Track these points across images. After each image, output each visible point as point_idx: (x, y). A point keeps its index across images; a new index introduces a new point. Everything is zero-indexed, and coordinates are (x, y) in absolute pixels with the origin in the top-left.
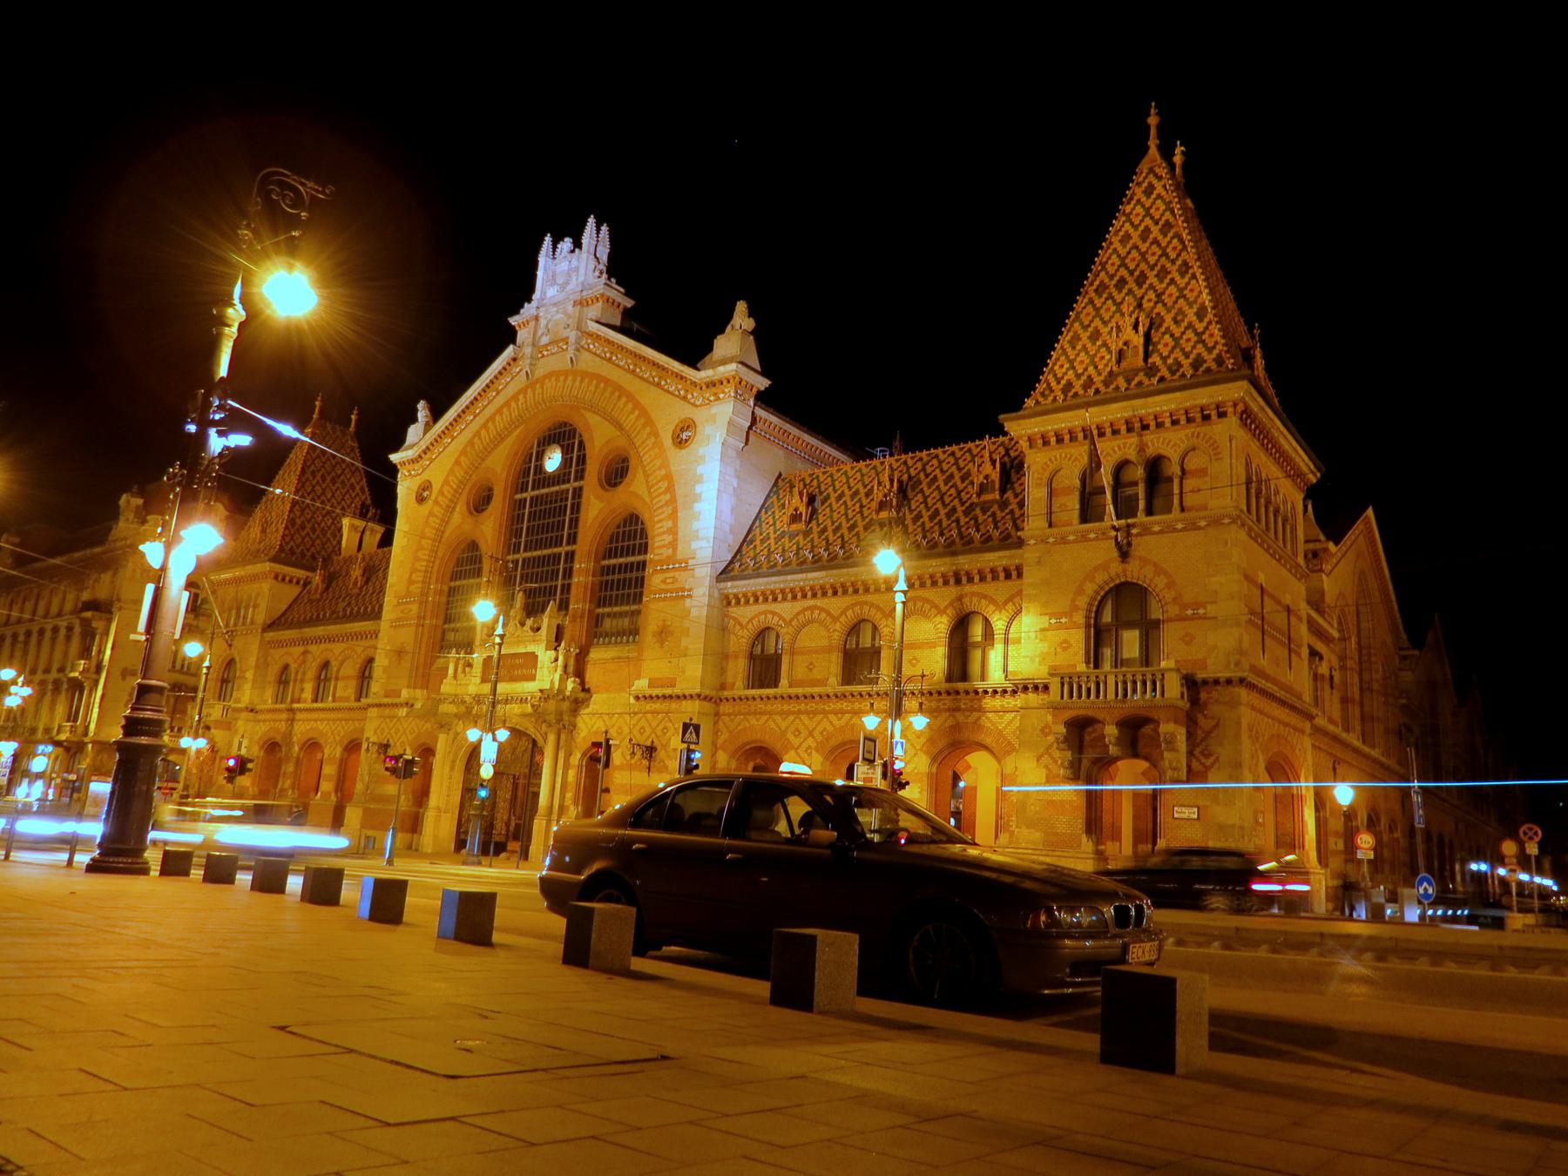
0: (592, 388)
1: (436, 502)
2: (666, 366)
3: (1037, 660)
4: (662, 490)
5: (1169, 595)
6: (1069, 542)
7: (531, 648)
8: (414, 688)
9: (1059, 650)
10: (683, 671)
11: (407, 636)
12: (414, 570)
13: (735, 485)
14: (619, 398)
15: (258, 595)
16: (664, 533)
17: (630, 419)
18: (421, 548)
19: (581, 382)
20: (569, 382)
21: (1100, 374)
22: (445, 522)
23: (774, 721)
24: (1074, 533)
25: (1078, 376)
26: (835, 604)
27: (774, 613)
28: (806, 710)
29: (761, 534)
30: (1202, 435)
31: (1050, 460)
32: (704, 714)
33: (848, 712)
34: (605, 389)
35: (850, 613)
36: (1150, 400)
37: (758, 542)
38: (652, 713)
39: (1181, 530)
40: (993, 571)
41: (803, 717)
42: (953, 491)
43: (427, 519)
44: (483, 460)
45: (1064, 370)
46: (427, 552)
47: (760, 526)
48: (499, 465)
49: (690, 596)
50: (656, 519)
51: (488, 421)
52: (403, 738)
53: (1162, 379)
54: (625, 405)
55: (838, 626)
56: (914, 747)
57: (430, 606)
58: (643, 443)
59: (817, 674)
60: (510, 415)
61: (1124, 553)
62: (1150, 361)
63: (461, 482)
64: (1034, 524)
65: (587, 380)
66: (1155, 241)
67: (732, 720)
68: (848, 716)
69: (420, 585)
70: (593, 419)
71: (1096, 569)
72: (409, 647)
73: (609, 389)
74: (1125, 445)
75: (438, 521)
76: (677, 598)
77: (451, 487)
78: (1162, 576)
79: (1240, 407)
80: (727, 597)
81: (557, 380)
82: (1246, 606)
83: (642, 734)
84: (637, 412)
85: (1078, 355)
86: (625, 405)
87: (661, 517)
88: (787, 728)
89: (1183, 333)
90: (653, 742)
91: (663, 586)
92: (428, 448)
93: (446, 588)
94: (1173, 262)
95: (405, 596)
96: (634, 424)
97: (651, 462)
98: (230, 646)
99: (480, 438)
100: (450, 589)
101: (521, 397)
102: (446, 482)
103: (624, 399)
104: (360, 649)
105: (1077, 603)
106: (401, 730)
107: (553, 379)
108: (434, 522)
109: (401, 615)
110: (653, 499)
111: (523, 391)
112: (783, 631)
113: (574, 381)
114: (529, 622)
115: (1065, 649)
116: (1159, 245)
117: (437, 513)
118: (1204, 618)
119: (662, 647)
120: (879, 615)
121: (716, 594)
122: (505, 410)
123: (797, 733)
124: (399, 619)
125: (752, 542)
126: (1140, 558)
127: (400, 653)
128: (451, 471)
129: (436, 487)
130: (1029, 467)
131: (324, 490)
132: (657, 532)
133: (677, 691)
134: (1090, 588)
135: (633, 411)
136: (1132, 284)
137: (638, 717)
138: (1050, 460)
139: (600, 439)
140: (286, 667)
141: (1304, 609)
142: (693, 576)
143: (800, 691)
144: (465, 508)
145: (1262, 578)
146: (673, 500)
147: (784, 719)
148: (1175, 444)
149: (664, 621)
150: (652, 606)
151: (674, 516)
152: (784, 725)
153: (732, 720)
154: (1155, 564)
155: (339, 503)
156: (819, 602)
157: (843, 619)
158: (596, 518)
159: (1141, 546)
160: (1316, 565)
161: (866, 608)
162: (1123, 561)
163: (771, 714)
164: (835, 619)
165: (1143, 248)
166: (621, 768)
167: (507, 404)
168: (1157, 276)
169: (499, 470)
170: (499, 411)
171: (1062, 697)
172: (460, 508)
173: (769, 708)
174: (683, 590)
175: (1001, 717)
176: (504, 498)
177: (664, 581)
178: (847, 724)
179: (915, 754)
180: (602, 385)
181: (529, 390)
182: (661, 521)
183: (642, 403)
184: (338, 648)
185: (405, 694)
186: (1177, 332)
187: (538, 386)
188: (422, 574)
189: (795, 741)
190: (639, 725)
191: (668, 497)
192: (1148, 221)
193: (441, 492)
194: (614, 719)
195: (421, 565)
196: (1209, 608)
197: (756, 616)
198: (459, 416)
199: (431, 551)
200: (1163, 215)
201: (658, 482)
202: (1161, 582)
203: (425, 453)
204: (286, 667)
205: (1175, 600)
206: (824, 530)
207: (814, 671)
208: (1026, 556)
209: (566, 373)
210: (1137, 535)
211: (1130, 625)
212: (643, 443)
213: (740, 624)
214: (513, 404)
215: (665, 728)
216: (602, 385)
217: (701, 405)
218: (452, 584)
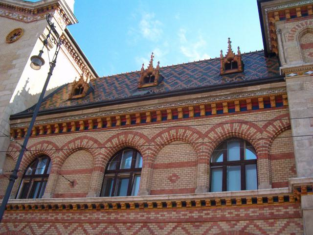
23: (31, 228)
26: (102, 136)
28: (63, 219)
33: (104, 222)
41: (58, 225)
68: (103, 225)
120: (142, 141)
143: (58, 201)
156: (89, 134)
161: (130, 136)
164: (101, 146)
173: (29, 216)
175: (272, 225)
178: (101, 233)
207: (76, 187)
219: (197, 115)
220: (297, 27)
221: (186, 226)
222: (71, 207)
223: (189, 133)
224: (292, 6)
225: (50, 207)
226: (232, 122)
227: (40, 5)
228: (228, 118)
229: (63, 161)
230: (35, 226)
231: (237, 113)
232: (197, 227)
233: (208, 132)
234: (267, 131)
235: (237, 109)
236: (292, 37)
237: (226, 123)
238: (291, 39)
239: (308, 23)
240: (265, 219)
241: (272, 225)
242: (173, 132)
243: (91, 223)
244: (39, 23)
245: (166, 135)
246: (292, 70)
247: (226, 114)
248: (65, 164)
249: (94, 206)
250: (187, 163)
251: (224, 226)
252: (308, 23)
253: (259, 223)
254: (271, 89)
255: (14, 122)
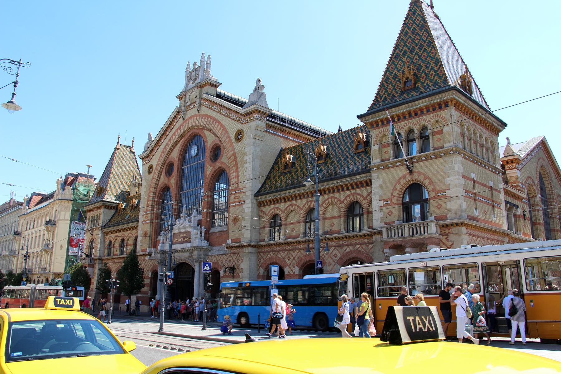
0: (206, 121)
1: (155, 173)
2: (231, 108)
3: (379, 220)
4: (233, 160)
5: (430, 187)
6: (389, 168)
7: (188, 229)
8: (151, 248)
9: (388, 215)
10: (244, 236)
11: (147, 227)
12: (148, 201)
13: (261, 155)
14: (216, 123)
15: (100, 214)
16: (234, 178)
17: (219, 132)
18: (150, 192)
19: (202, 119)
20: (198, 119)
21: (397, 93)
22: (158, 180)
23: (280, 254)
24: (391, 163)
25: (389, 95)
26: (301, 203)
27: (278, 208)
28: (292, 248)
29: (273, 175)
30: (439, 115)
31: (380, 132)
32: (252, 253)
34: (210, 120)
35: (306, 206)
36: (416, 102)
37: (272, 178)
38: (233, 253)
39: (433, 158)
40: (361, 182)
41: (291, 252)
42: (347, 149)
43: (152, 180)
44: (170, 154)
45: (383, 93)
46: (152, 193)
47: (273, 171)
48: (175, 155)
49: (244, 204)
50: (231, 172)
51: (170, 138)
52: (148, 268)
53: (422, 93)
54: (218, 126)
55: (302, 212)
56: (334, 262)
57: (155, 214)
58: (225, 141)
59: (295, 233)
60: (178, 135)
61: (411, 172)
62: (417, 85)
63: (162, 164)
64: (376, 161)
65: (204, 118)
66: (418, 34)
67: (264, 255)
69: (151, 207)
70: (207, 133)
71: (400, 178)
72: (148, 232)
73: (212, 120)
74: (408, 122)
75: (155, 180)
76: (240, 205)
77: (159, 166)
78: (427, 179)
79: (454, 102)
80: (260, 202)
81: (194, 119)
82: (464, 189)
83: (230, 262)
84: (222, 129)
85: (388, 86)
86: (218, 126)
87: (233, 171)
88: (285, 257)
89: (430, 72)
90: (234, 266)
91: (235, 200)
92: (151, 151)
93: (160, 207)
94: (425, 42)
95: (146, 211)
96: (221, 134)
97: (228, 149)
98: (92, 235)
99: (168, 146)
100: (162, 207)
101: (181, 127)
102: (158, 164)
103: (217, 124)
104: (133, 232)
105: (394, 194)
106: (147, 265)
107: (192, 118)
108: (155, 181)
109: (146, 219)
110: (229, 164)
111: (182, 125)
112: (282, 215)
113: (199, 119)
114: (187, 219)
115: (390, 215)
116: (419, 35)
117: (155, 177)
118: (445, 197)
119: (235, 226)
121: (255, 202)
122: (176, 133)
123: (289, 259)
124: (144, 221)
125: (270, 178)
126: (418, 172)
127: (145, 235)
128: (159, 160)
129: (154, 167)
130: (371, 136)
131: (122, 171)
132: (231, 178)
133: (241, 244)
134: (398, 187)
135: (220, 128)
136: (409, 53)
137: (229, 255)
138: (380, 132)
139: (210, 140)
140: (111, 241)
141: (501, 186)
142: (245, 195)
143: (288, 241)
144: (165, 174)
145: (473, 176)
146: (236, 164)
147: (284, 253)
148: (429, 121)
149: (235, 215)
150: (231, 209)
151: (237, 171)
152: (284, 255)
153: (264, 255)
154: (424, 174)
155: (128, 176)
156: (294, 202)
157: (304, 208)
158: (210, 174)
159: (418, 167)
160: (513, 166)
162: (411, 174)
163: (279, 251)
164: (301, 209)
165: (413, 37)
166: (223, 277)
167: (177, 130)
168: (418, 48)
169: (175, 157)
170: (174, 134)
171: (388, 237)
172: (163, 175)
173: (278, 248)
174: (242, 201)
175: (368, 246)
176: (178, 168)
177: (235, 198)
179: (335, 265)
180: (209, 119)
181: (184, 124)
182: (232, 173)
183: (224, 124)
184: (127, 233)
185: (148, 250)
186: (427, 71)
187: (187, 122)
188: (151, 202)
189: (288, 262)
190: (229, 259)
191: (234, 163)
192: (414, 26)
193: (156, 169)
194: (220, 257)
195: (151, 198)
196: (447, 191)
197: (271, 210)
198: (161, 137)
199: (154, 192)
200: (420, 22)
201: (230, 157)
202: (426, 182)
203: (150, 154)
204: (111, 241)
205: (433, 190)
206: (297, 171)
208: (372, 175)
209: (196, 116)
210: (416, 162)
211: (416, 203)
212: (225, 141)
213: (265, 214)
214: (179, 130)
215: (238, 260)
216: (209, 119)
217: (245, 123)
218: (163, 205)
219: (338, 191)
220: (379, 133)
221: (338, 248)
222: (294, 243)
223: (336, 200)
224: (375, 119)
225: (285, 243)
226: (354, 194)
227: (246, 111)
228: (351, 192)
229: (286, 218)
230: (281, 252)
231: (355, 189)
232: (342, 248)
233: (344, 200)
234: (367, 199)
235: (355, 187)
236: (376, 141)
237: (351, 194)
238: (375, 144)
239: (385, 130)
240: (365, 244)
241: (368, 246)
242: (330, 200)
243: (303, 249)
244: (250, 124)
245: (327, 202)
246: (374, 167)
247: (350, 190)
248: (288, 220)
249: (302, 242)
250: (337, 216)
251: (351, 248)
252: (385, 130)
253: (363, 246)
254: (366, 177)
255: (257, 198)
